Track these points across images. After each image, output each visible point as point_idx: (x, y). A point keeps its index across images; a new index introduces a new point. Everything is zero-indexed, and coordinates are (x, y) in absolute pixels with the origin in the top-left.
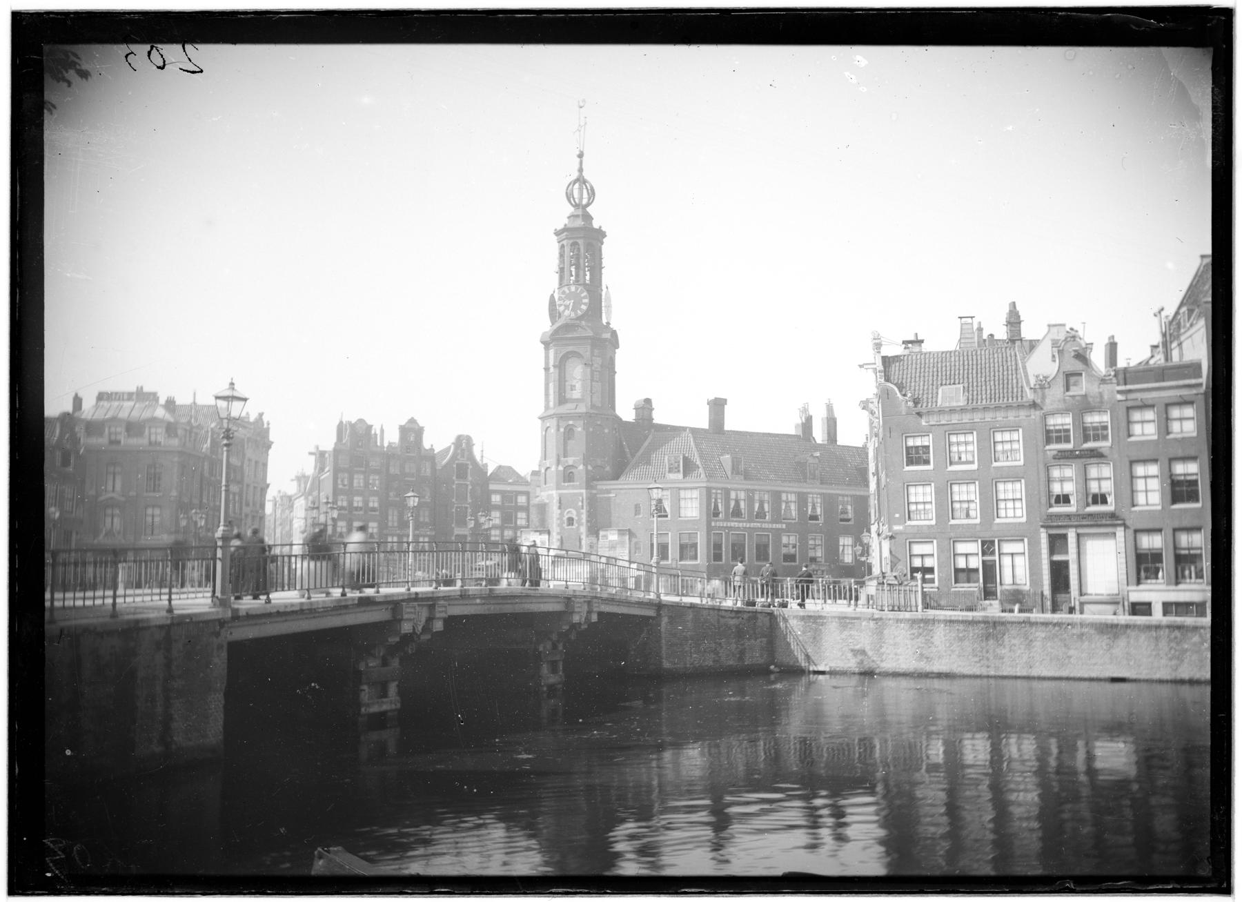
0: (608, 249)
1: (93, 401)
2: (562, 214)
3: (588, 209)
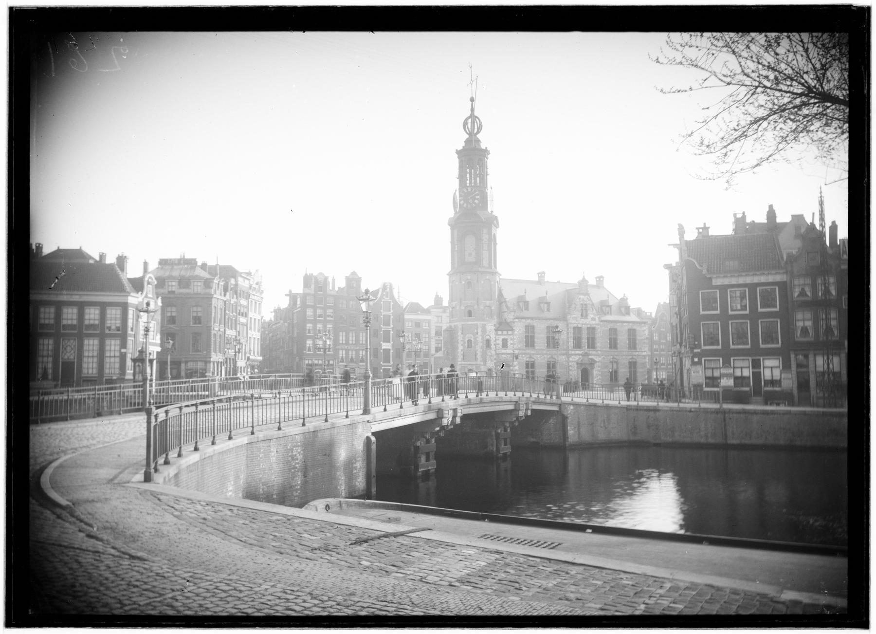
0: (491, 162)
1: (156, 265)
2: (460, 139)
3: (478, 136)
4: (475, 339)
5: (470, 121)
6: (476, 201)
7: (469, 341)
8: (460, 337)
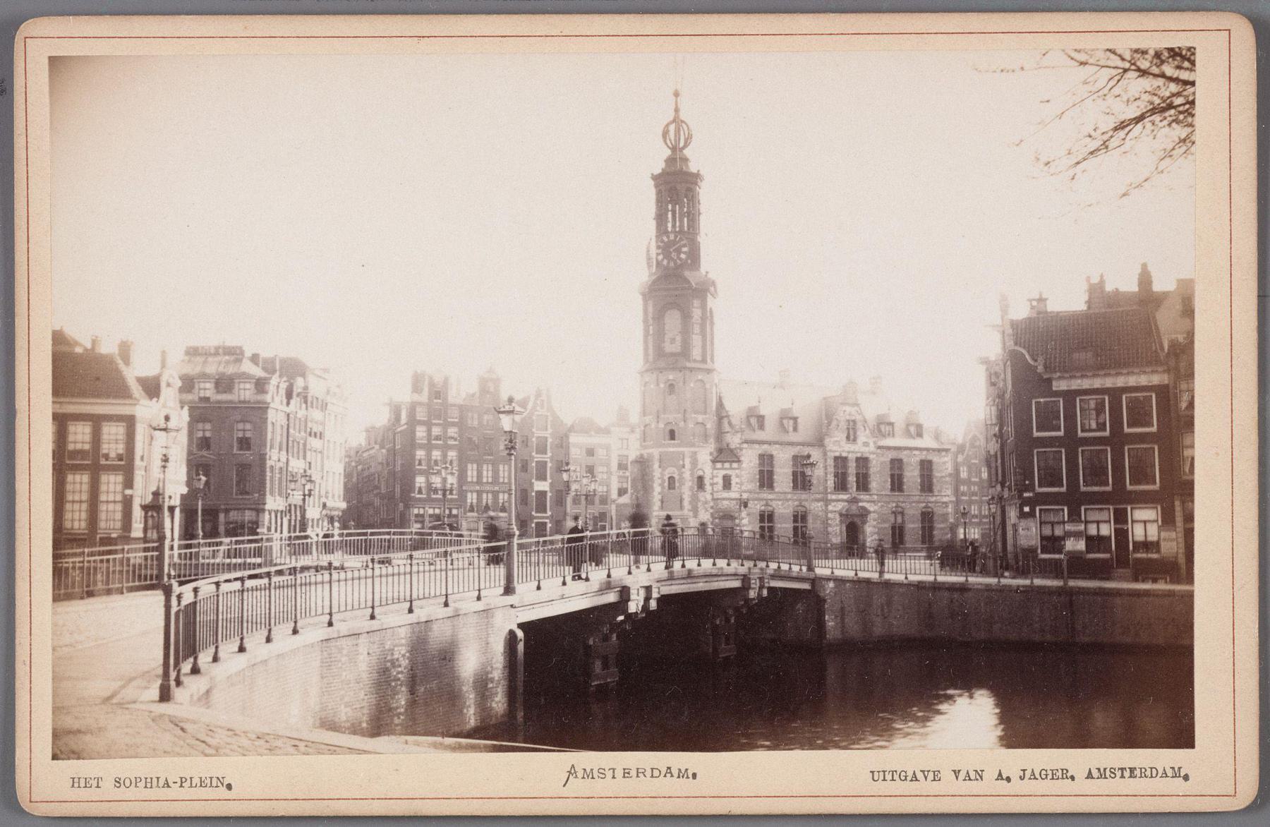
0: (706, 194)
3: (686, 152)
4: (681, 474)
5: (672, 128)
6: (683, 256)
7: (671, 479)
8: (657, 472)
